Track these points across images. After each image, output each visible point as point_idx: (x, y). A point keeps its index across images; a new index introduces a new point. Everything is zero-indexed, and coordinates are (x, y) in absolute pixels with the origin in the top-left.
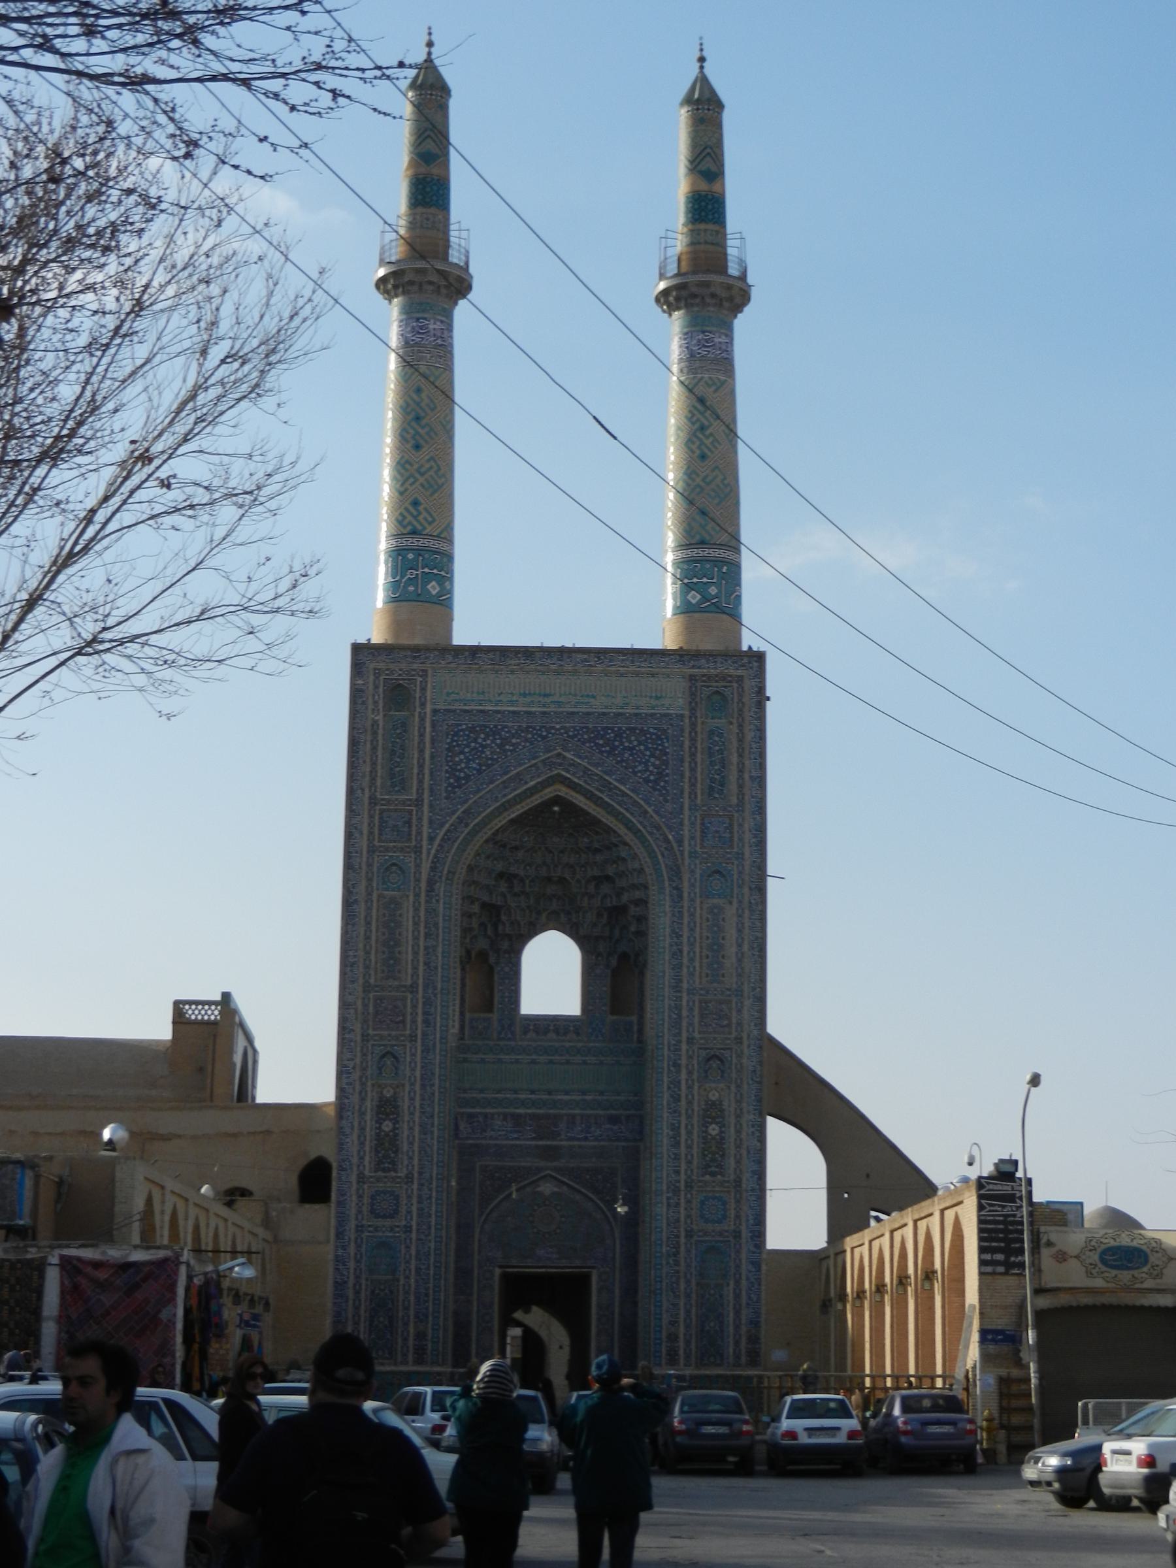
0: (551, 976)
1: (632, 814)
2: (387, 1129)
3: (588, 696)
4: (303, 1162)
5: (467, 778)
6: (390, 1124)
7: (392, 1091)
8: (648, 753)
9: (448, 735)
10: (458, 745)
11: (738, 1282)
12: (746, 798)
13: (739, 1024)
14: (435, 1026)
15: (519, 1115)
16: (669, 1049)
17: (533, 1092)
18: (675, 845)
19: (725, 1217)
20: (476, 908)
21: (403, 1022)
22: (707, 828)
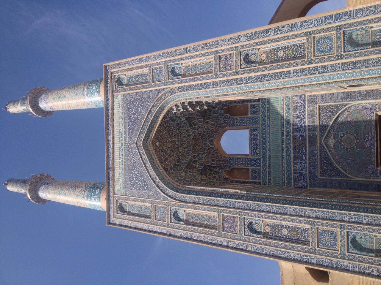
0: (235, 142)
1: (154, 112)
2: (287, 232)
3: (119, 133)
4: (310, 276)
5: (144, 182)
6: (284, 229)
7: (267, 227)
8: (135, 107)
9: (132, 189)
10: (135, 185)
11: (370, 21)
12: (146, 64)
13: (229, 50)
14: (236, 202)
15: (294, 156)
16: (242, 83)
17: (283, 150)
18: (164, 92)
19: (328, 38)
20: (199, 177)
21: (234, 218)
22: (157, 78)
